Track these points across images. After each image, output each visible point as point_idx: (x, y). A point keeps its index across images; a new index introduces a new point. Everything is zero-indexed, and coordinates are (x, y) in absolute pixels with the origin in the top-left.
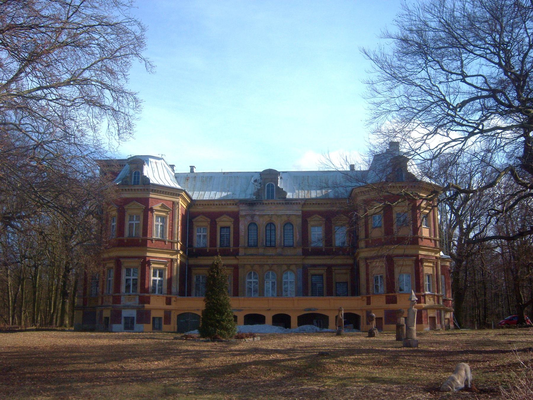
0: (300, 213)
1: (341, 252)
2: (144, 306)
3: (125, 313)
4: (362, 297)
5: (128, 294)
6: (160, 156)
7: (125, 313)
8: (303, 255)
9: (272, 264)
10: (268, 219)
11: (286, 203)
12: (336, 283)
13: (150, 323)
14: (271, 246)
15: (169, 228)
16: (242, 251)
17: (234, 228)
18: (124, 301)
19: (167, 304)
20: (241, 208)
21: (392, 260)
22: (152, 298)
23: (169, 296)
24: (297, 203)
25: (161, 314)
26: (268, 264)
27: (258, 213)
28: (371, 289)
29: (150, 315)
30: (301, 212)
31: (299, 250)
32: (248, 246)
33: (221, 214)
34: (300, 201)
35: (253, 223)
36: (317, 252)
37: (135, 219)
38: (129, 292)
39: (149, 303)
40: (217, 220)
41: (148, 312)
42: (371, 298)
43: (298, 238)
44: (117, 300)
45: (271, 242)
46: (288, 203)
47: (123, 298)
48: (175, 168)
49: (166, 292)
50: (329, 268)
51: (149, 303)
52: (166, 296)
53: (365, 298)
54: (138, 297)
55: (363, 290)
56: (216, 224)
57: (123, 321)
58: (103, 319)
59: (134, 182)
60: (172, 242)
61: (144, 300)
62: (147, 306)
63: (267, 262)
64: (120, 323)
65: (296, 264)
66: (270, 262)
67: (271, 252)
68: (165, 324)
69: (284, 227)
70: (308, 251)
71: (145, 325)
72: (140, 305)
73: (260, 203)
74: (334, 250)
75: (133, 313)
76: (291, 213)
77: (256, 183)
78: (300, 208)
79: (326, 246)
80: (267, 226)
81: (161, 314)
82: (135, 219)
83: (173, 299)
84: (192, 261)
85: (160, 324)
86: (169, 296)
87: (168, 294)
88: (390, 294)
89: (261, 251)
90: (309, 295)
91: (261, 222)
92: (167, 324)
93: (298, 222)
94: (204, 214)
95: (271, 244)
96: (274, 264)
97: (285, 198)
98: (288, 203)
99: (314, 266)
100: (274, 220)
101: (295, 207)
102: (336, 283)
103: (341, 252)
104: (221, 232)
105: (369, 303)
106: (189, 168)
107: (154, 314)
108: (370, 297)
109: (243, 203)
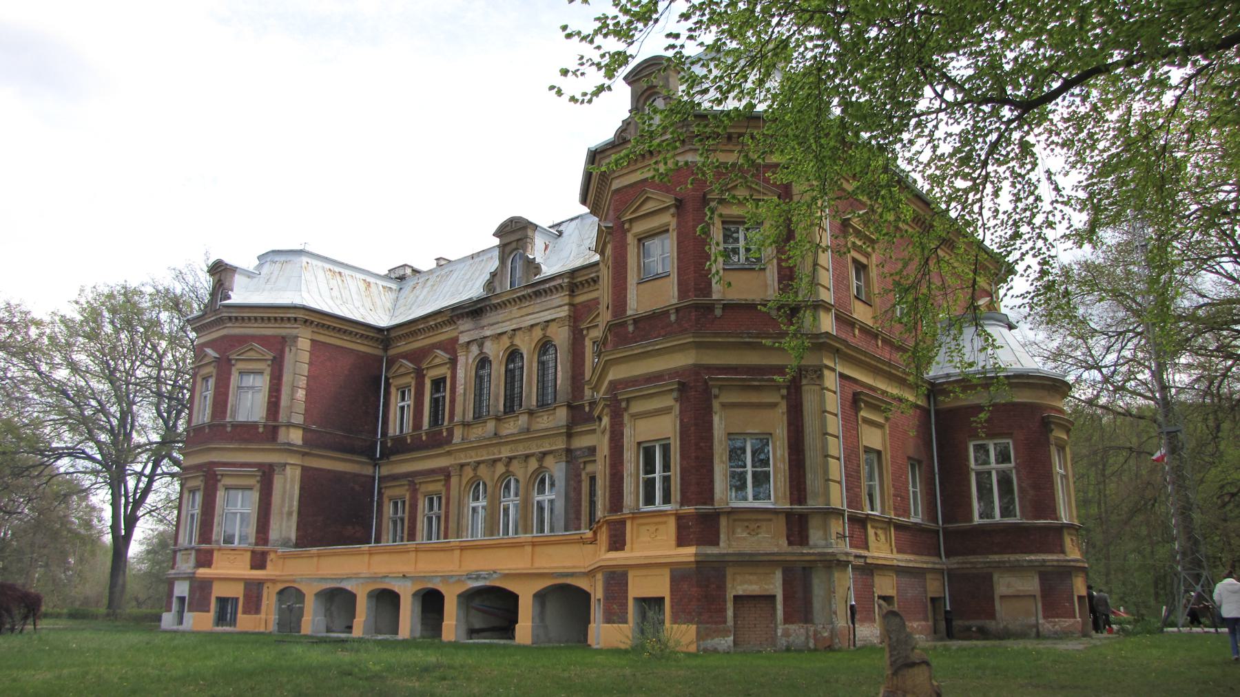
0: (564, 312)
15: (270, 396)
19: (253, 567)
20: (462, 328)
23: (260, 548)
25: (237, 591)
27: (488, 333)
31: (562, 415)
34: (559, 281)
35: (483, 362)
51: (208, 564)
54: (193, 552)
57: (175, 605)
62: (202, 572)
63: (500, 453)
66: (505, 452)
68: (244, 613)
76: (549, 318)
78: (566, 300)
81: (237, 591)
84: (385, 471)
85: (235, 613)
86: (260, 548)
87: (257, 544)
91: (495, 351)
93: (561, 336)
94: (406, 356)
96: (515, 457)
107: (219, 591)
109: (461, 316)
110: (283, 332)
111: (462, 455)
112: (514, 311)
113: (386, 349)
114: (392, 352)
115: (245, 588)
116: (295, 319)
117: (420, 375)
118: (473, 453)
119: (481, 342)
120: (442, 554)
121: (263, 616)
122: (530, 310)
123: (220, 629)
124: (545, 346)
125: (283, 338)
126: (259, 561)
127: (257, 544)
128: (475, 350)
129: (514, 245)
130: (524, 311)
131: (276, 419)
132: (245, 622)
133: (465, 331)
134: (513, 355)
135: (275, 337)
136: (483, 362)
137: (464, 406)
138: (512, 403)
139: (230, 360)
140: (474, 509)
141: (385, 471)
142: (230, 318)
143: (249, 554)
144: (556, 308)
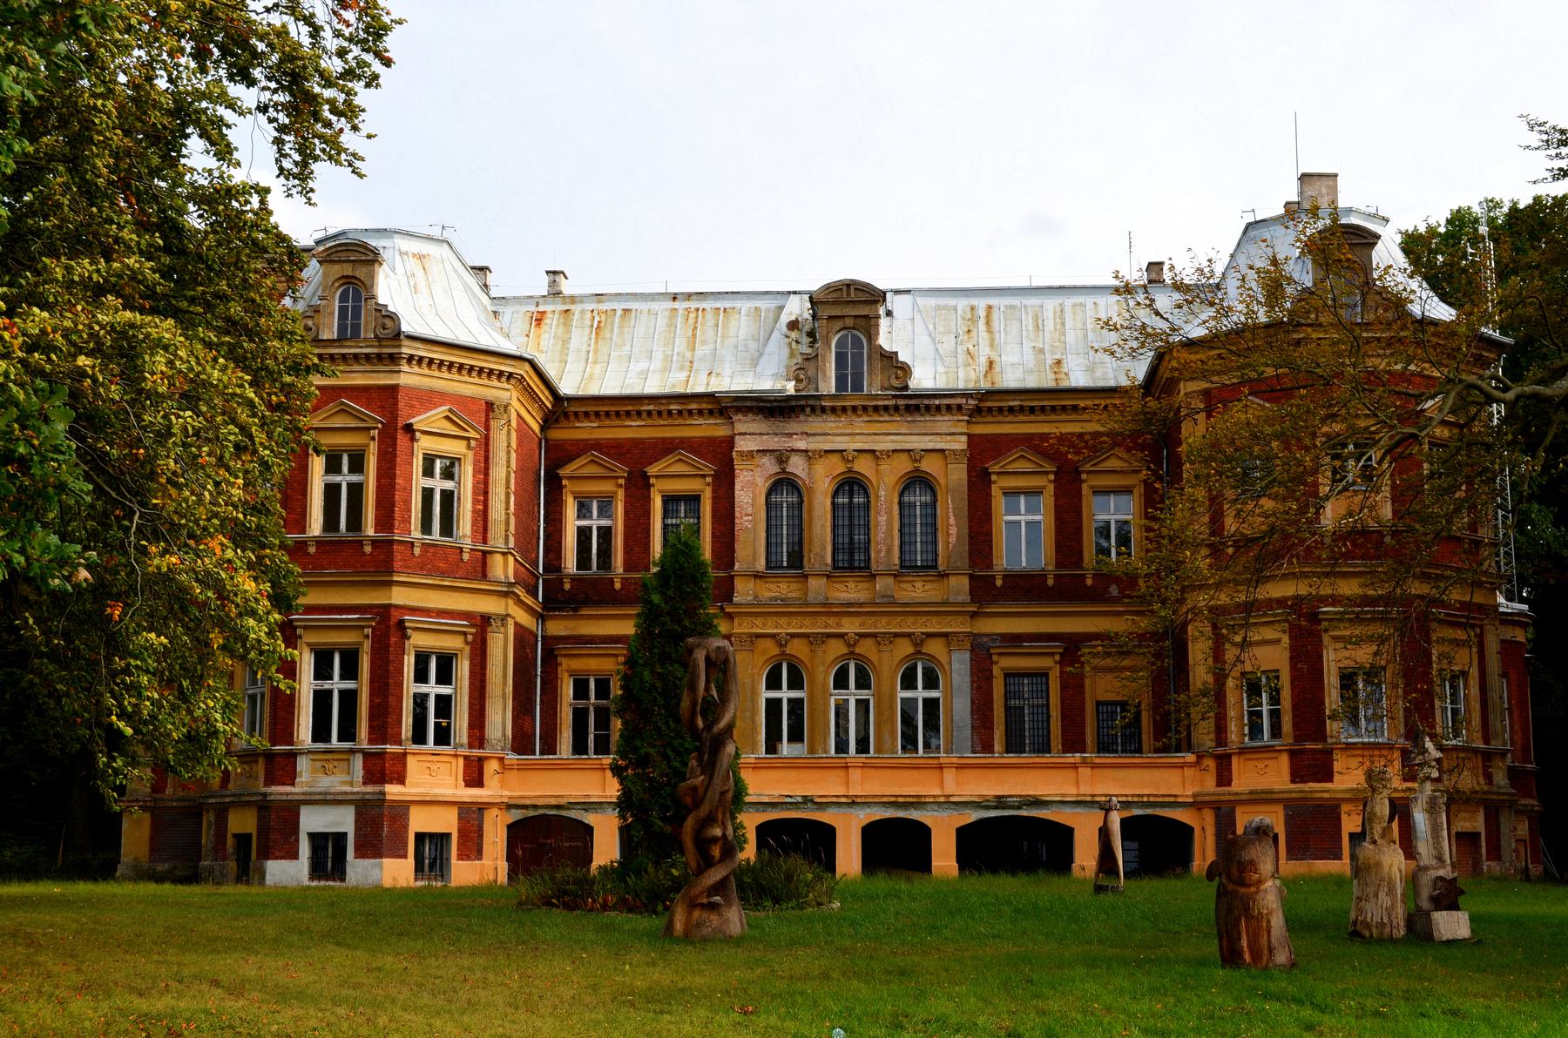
0: (960, 444)
1: (1114, 590)
2: (384, 794)
3: (313, 821)
4: (1200, 757)
5: (320, 746)
6: (436, 232)
7: (313, 821)
8: (973, 601)
9: (861, 635)
10: (841, 468)
11: (908, 408)
12: (1098, 704)
13: (405, 856)
14: (851, 568)
15: (475, 502)
16: (744, 591)
17: (715, 499)
18: (308, 776)
19: (469, 784)
20: (739, 427)
21: (1314, 618)
22: (410, 761)
23: (476, 752)
24: (949, 407)
25: (446, 822)
26: (841, 636)
27: (801, 444)
28: (1233, 727)
29: (406, 827)
30: (964, 438)
31: (959, 586)
32: (768, 567)
33: (667, 448)
36: (1025, 588)
37: (345, 469)
38: (328, 739)
39: (401, 780)
40: (652, 470)
41: (402, 809)
42: (1234, 760)
43: (952, 540)
44: (282, 766)
45: (851, 553)
46: (917, 408)
47: (303, 764)
48: (491, 279)
49: (465, 740)
50: (1071, 646)
51: (401, 780)
52: (465, 751)
53: (1210, 763)
55: (1204, 735)
56: (648, 486)
57: (305, 848)
58: (230, 841)
59: (342, 328)
60: (485, 553)
61: (383, 769)
62: (393, 791)
63: (839, 625)
64: (294, 855)
65: (945, 635)
67: (851, 591)
68: (460, 857)
69: (901, 494)
70: (991, 590)
71: (386, 861)
72: (370, 789)
73: (813, 409)
74: (1089, 582)
75: (342, 821)
76: (930, 446)
77: (794, 335)
79: (1059, 565)
80: (836, 494)
82: (345, 469)
83: (491, 767)
84: (557, 628)
86: (476, 752)
87: (471, 746)
88: (1309, 746)
89: (816, 584)
90: (997, 747)
92: (468, 858)
93: (954, 477)
94: (598, 445)
95: (851, 560)
97: (906, 388)
98: (917, 408)
99: (1014, 641)
100: (864, 466)
101: (944, 423)
102: (1098, 704)
103: (1114, 590)
104: (665, 515)
105: (1224, 778)
106: (546, 279)
107: (420, 821)
108: (1229, 756)
109: (750, 409)
110: (491, 394)
111: (759, 621)
112: (860, 424)
113: (543, 429)
114: (557, 434)
115: (460, 818)
116: (510, 375)
117: (638, 487)
118: (782, 621)
119: (782, 457)
120: (915, 773)
121: (487, 861)
122: (891, 428)
123: (315, 883)
124: (917, 481)
125: (490, 406)
126: (474, 777)
127: (471, 746)
128: (769, 466)
129: (849, 322)
130: (877, 428)
131: (485, 542)
132: (463, 873)
133: (750, 436)
134: (851, 484)
135: (473, 400)
136: (784, 483)
137: (751, 546)
138: (852, 557)
139: (409, 429)
140: (773, 705)
141: (557, 628)
142: (411, 358)
143: (461, 761)
144: (950, 435)
